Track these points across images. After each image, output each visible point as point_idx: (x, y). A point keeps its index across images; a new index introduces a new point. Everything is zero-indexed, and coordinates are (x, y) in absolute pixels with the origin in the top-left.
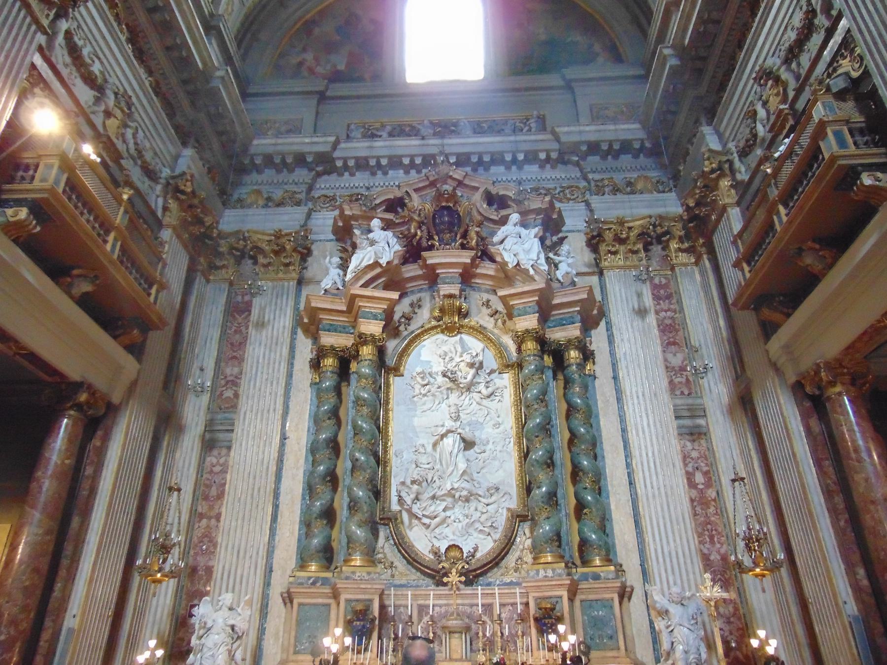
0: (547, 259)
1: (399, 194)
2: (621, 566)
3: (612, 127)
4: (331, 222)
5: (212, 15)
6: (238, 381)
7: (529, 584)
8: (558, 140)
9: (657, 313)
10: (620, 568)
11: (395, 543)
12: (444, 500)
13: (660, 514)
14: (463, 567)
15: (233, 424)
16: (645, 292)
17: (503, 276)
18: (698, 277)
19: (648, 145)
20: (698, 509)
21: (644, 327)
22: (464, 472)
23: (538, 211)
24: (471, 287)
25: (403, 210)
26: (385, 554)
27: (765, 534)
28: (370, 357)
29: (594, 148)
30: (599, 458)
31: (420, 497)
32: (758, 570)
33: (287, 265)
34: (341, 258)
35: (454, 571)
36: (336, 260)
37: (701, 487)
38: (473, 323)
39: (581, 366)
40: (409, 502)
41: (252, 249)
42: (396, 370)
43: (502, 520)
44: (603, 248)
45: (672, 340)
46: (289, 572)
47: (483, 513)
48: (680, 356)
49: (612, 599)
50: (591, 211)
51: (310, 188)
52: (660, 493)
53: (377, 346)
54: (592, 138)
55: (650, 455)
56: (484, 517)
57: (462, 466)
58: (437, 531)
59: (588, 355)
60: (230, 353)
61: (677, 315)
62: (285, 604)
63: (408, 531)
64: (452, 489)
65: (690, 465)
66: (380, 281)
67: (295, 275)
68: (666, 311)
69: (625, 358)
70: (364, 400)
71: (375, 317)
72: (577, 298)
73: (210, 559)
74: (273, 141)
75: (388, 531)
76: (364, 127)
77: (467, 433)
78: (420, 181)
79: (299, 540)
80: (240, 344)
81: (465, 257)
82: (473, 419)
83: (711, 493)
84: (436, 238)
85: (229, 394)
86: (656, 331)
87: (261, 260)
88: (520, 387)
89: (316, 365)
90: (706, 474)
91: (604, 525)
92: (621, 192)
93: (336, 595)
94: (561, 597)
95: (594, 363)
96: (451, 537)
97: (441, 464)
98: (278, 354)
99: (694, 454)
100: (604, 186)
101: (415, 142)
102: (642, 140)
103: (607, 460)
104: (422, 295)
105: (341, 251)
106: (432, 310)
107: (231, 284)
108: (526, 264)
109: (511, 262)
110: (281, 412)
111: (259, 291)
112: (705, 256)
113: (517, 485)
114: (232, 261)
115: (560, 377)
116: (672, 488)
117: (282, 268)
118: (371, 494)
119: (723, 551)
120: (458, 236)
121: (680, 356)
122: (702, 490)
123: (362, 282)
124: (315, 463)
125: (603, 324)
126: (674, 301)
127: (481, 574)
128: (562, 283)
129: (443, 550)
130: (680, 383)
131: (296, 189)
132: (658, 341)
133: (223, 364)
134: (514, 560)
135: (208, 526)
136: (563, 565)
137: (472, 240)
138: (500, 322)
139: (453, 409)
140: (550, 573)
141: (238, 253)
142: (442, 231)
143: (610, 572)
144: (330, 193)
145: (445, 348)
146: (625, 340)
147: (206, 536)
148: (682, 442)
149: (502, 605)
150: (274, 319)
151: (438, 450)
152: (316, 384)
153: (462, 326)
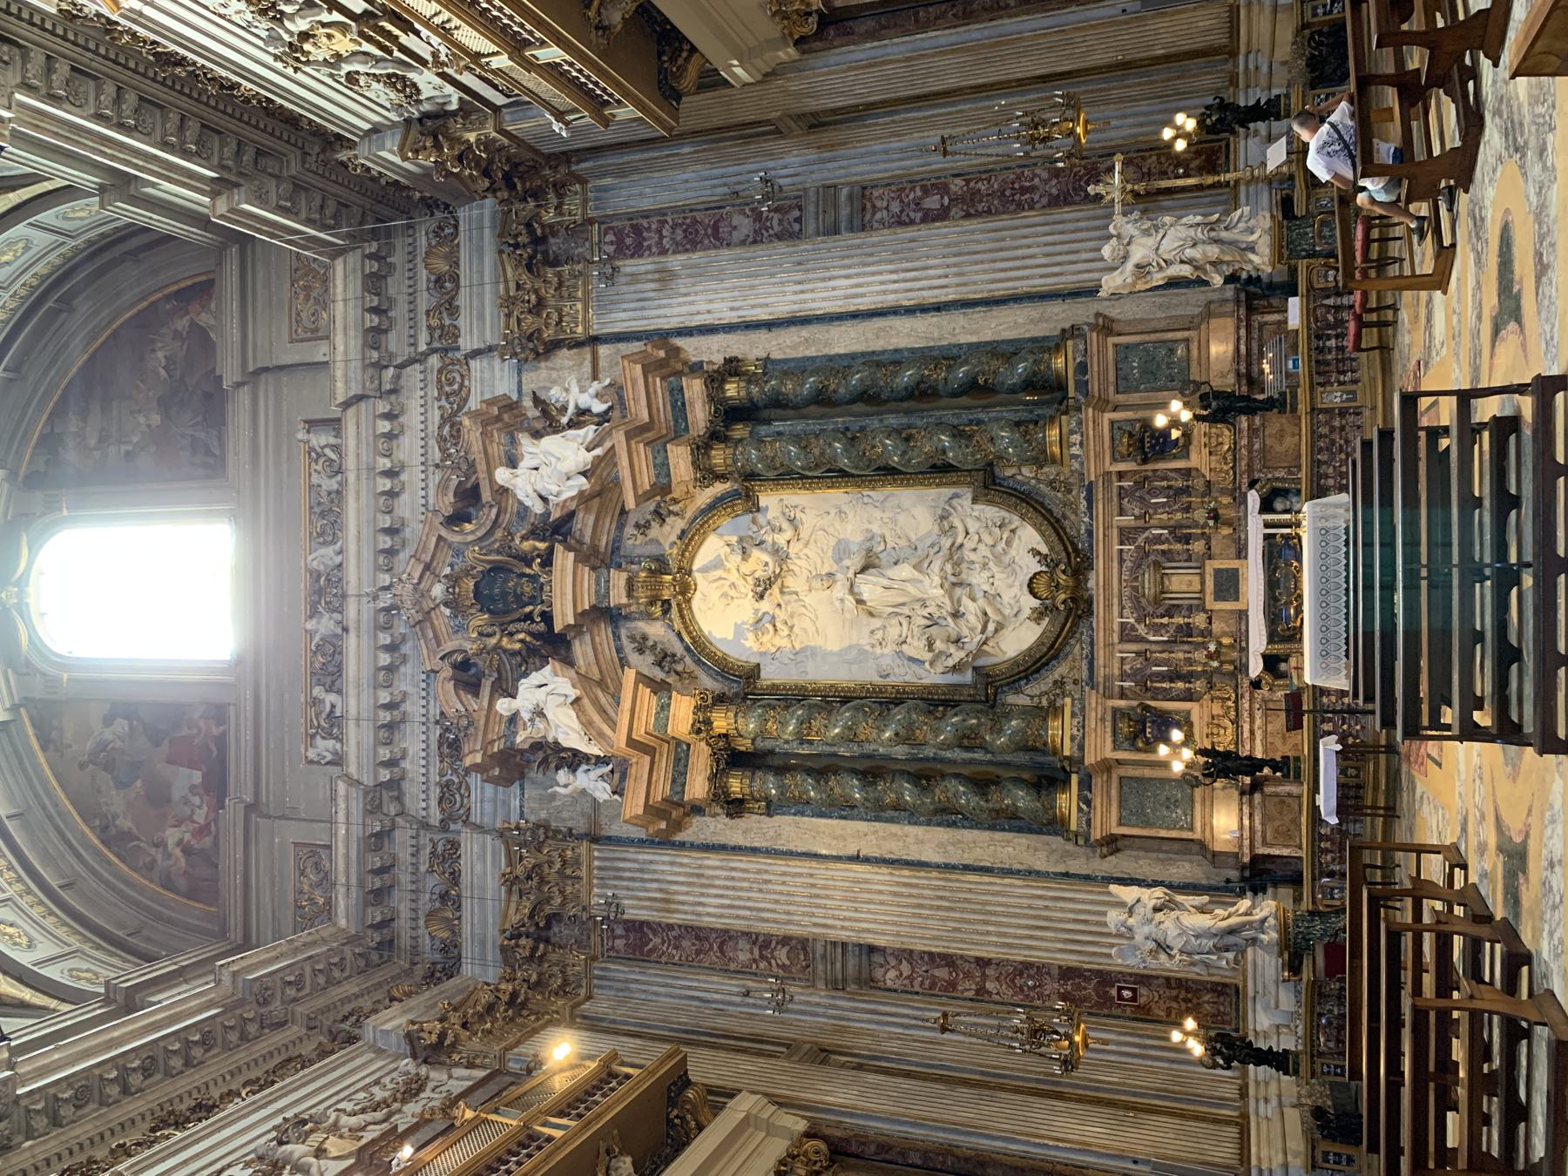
0: (572, 425)
1: (447, 672)
2: (1064, 330)
3: (340, 306)
4: (489, 788)
5: (107, 1000)
6: (761, 939)
8: (359, 398)
9: (664, 252)
10: (1073, 332)
11: (1026, 677)
12: (959, 601)
13: (986, 266)
14: (1064, 572)
15: (834, 944)
16: (628, 270)
17: (597, 500)
18: (607, 181)
19: (373, 247)
21: (690, 276)
22: (917, 567)
25: (475, 665)
26: (1040, 696)
27: (1025, 114)
28: (731, 714)
29: (374, 337)
31: (954, 637)
32: (1079, 130)
34: (558, 768)
36: (563, 776)
38: (675, 551)
39: (751, 379)
40: (962, 654)
43: (992, 513)
46: (1070, 847)
47: (980, 540)
48: (737, 220)
49: (1116, 345)
50: (490, 349)
51: (425, 825)
52: (955, 265)
53: (713, 704)
54: (355, 343)
55: (894, 277)
56: (988, 540)
58: (1007, 612)
59: (733, 367)
60: (713, 957)
62: (1118, 850)
65: (912, 215)
67: (584, 847)
68: (661, 237)
69: (738, 309)
71: (664, 708)
72: (641, 382)
73: (1048, 973)
74: (341, 890)
76: (313, 737)
77: (855, 562)
78: (424, 635)
79: (1020, 830)
81: (564, 560)
82: (830, 553)
83: (957, 185)
84: (528, 609)
85: (782, 954)
86: (696, 257)
88: (786, 477)
89: (736, 807)
90: (926, 191)
91: (1005, 351)
92: (453, 298)
93: (1107, 766)
94: (1112, 423)
96: (1015, 590)
97: (903, 604)
98: (718, 873)
99: (895, 207)
100: (442, 327)
101: (351, 642)
102: (365, 256)
103: (902, 345)
104: (623, 632)
106: (649, 617)
108: (585, 458)
110: (814, 864)
111: (613, 904)
112: (574, 168)
113: (938, 485)
114: (553, 957)
115: (766, 413)
116: (947, 246)
119: (1045, 175)
121: (737, 220)
124: (898, 807)
125: (679, 342)
126: (645, 223)
127: (1074, 545)
129: (1036, 603)
131: (428, 851)
132: (712, 252)
133: (732, 966)
135: (997, 979)
136: (1064, 418)
137: (536, 548)
139: (817, 584)
140: (1076, 438)
143: (1075, 346)
144: (435, 793)
145: (715, 596)
146: (709, 307)
147: (1013, 981)
148: (876, 225)
149: (1122, 512)
150: (657, 881)
152: (768, 806)
153: (680, 569)
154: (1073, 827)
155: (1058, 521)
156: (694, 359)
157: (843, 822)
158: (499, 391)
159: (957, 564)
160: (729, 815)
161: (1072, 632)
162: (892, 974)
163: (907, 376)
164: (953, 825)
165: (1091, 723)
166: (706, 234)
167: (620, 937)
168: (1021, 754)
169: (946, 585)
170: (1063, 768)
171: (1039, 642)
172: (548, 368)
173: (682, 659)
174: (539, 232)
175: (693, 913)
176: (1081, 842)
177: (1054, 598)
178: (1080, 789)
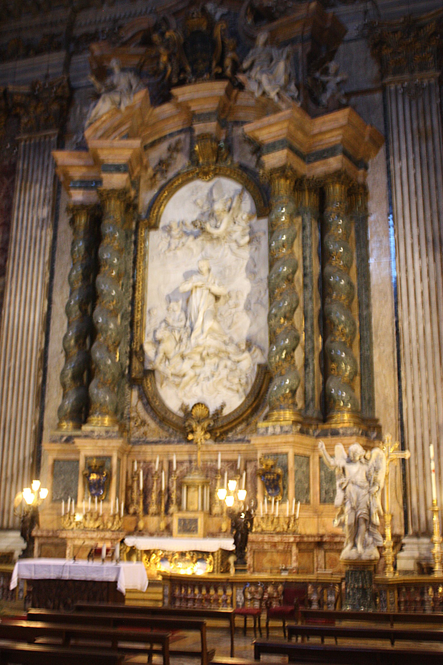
14: (209, 425)
35: (199, 429)
84: (189, 69)
94: (287, 454)
120: (214, 64)
125: (382, 151)
140: (278, 430)
144: (92, 29)
156: (370, 162)
159: (216, 355)
165: (100, 443)
171: (167, 410)
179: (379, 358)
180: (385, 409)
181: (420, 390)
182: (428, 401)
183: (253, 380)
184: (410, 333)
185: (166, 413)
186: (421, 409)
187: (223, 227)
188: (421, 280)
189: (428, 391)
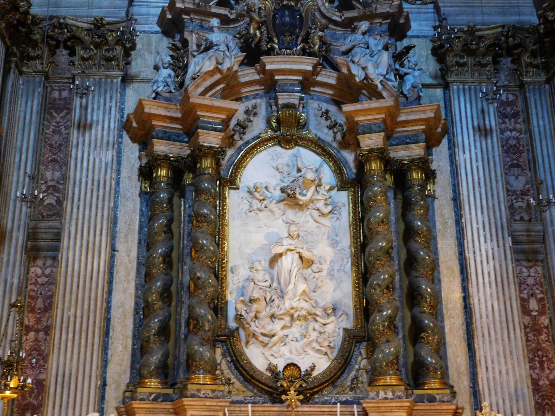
4: (158, 11)
6: (61, 187)
7: (370, 405)
9: (502, 132)
12: (282, 319)
14: (301, 386)
20: (530, 335)
23: (385, 16)
24: (309, 94)
30: (436, 281)
31: (258, 315)
33: (109, 60)
34: (172, 56)
37: (534, 313)
40: (249, 320)
41: (69, 39)
42: (232, 183)
43: (338, 341)
44: (451, 59)
45: (515, 162)
46: (123, 387)
47: (320, 333)
48: (522, 179)
57: (302, 287)
58: (275, 348)
59: (430, 175)
60: (49, 156)
61: (522, 136)
63: (245, 348)
64: (292, 308)
65: (525, 292)
66: (219, 88)
68: (511, 131)
70: (205, 216)
72: (423, 116)
75: (225, 348)
79: (133, 355)
80: (60, 145)
85: (50, 200)
87: (80, 52)
95: (434, 184)
96: (288, 355)
97: (279, 283)
99: (530, 281)
103: (443, 284)
104: (258, 101)
105: (171, 49)
107: (47, 78)
109: (358, 74)
113: (355, 306)
115: (400, 196)
117: (104, 63)
118: (212, 312)
120: (300, 39)
121: (522, 179)
122: (535, 316)
123: (201, 90)
125: (445, 141)
127: (317, 393)
128: (407, 98)
129: (280, 368)
130: (520, 207)
133: (42, 168)
134: (350, 378)
136: (403, 387)
137: (315, 45)
138: (339, 137)
140: (390, 395)
141: (54, 43)
142: (283, 33)
143: (446, 395)
148: (519, 268)
151: (276, 268)
154: (139, 390)
155: (333, 383)
157: (136, 241)
158: (413, 25)
159: (305, 318)
160: (141, 169)
161: (262, 390)
162: (39, 271)
163: (426, 288)
164: (136, 312)
166: (513, 159)
167: (60, 95)
168: (185, 357)
169: (292, 311)
170: (176, 384)
172: (427, 56)
173: (241, 139)
174: (516, 51)
175: (78, 143)
176: (127, 394)
177: (284, 379)
178: (164, 395)
179: (450, 329)
180: (458, 377)
181: (493, 362)
182: (500, 372)
183: (340, 344)
184: (480, 309)
185: (255, 372)
186: (494, 378)
187: (309, 194)
188: (488, 263)
189: (499, 363)
